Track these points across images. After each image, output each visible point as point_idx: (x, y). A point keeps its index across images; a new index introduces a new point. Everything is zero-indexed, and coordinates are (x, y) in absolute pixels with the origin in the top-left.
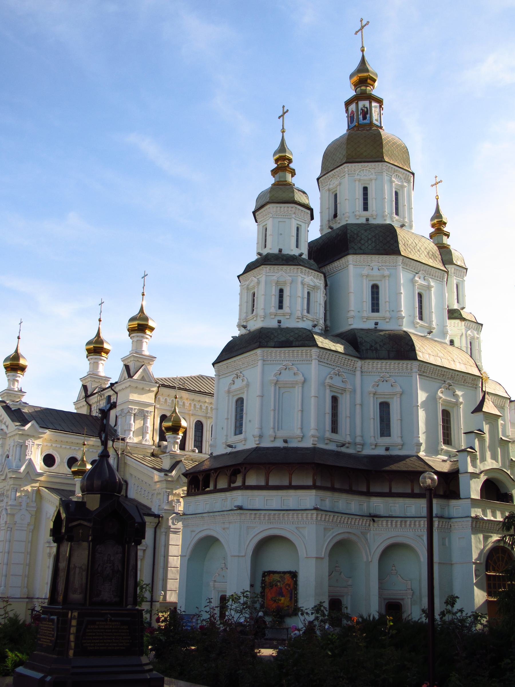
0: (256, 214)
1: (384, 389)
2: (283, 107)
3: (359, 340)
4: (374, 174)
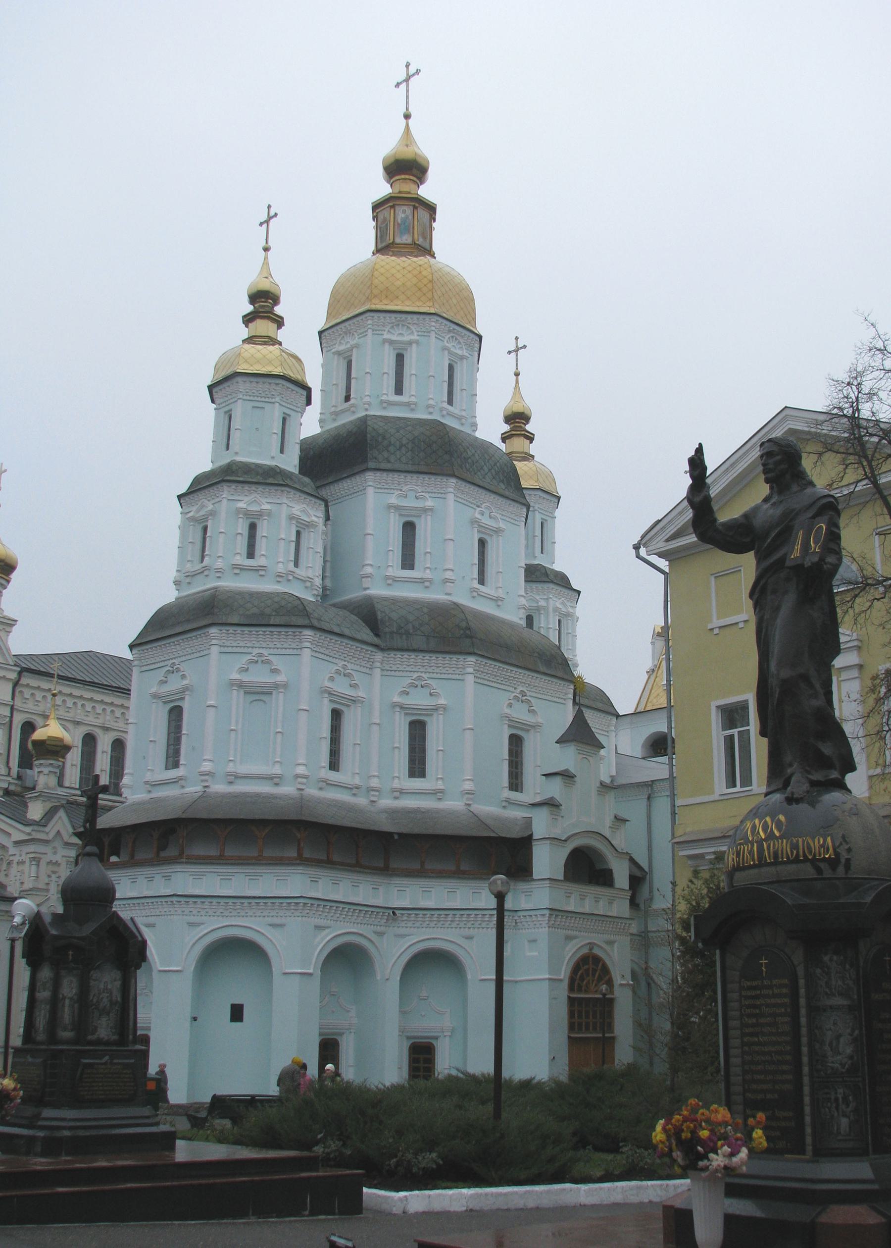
0: (214, 390)
1: (419, 699)
2: (269, 207)
3: (380, 616)
4: (416, 333)
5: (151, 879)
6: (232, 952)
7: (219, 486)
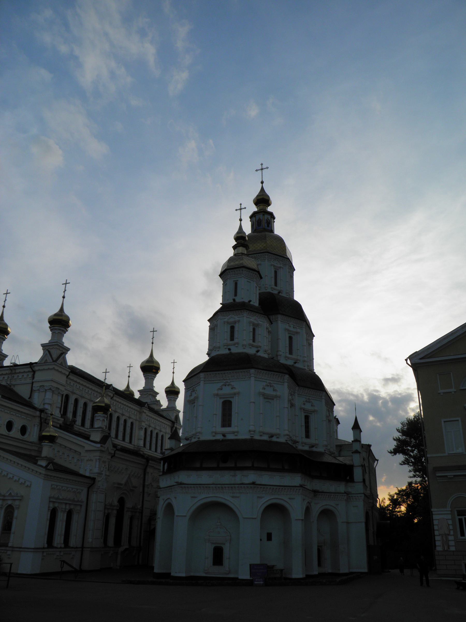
0: (228, 271)
1: (308, 407)
2: (241, 204)
6: (276, 510)
7: (242, 311)
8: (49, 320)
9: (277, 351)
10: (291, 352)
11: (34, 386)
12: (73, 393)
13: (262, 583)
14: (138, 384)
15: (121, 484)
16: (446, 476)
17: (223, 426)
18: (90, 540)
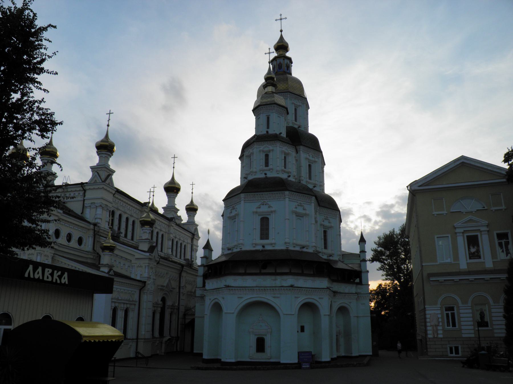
0: (261, 107)
1: (326, 223)
5: (275, 280)
6: (309, 307)
8: (96, 145)
9: (300, 177)
10: (310, 178)
11: (85, 202)
12: (118, 209)
13: (308, 366)
14: (160, 201)
15: (164, 286)
16: (438, 281)
17: (262, 238)
18: (143, 333)
